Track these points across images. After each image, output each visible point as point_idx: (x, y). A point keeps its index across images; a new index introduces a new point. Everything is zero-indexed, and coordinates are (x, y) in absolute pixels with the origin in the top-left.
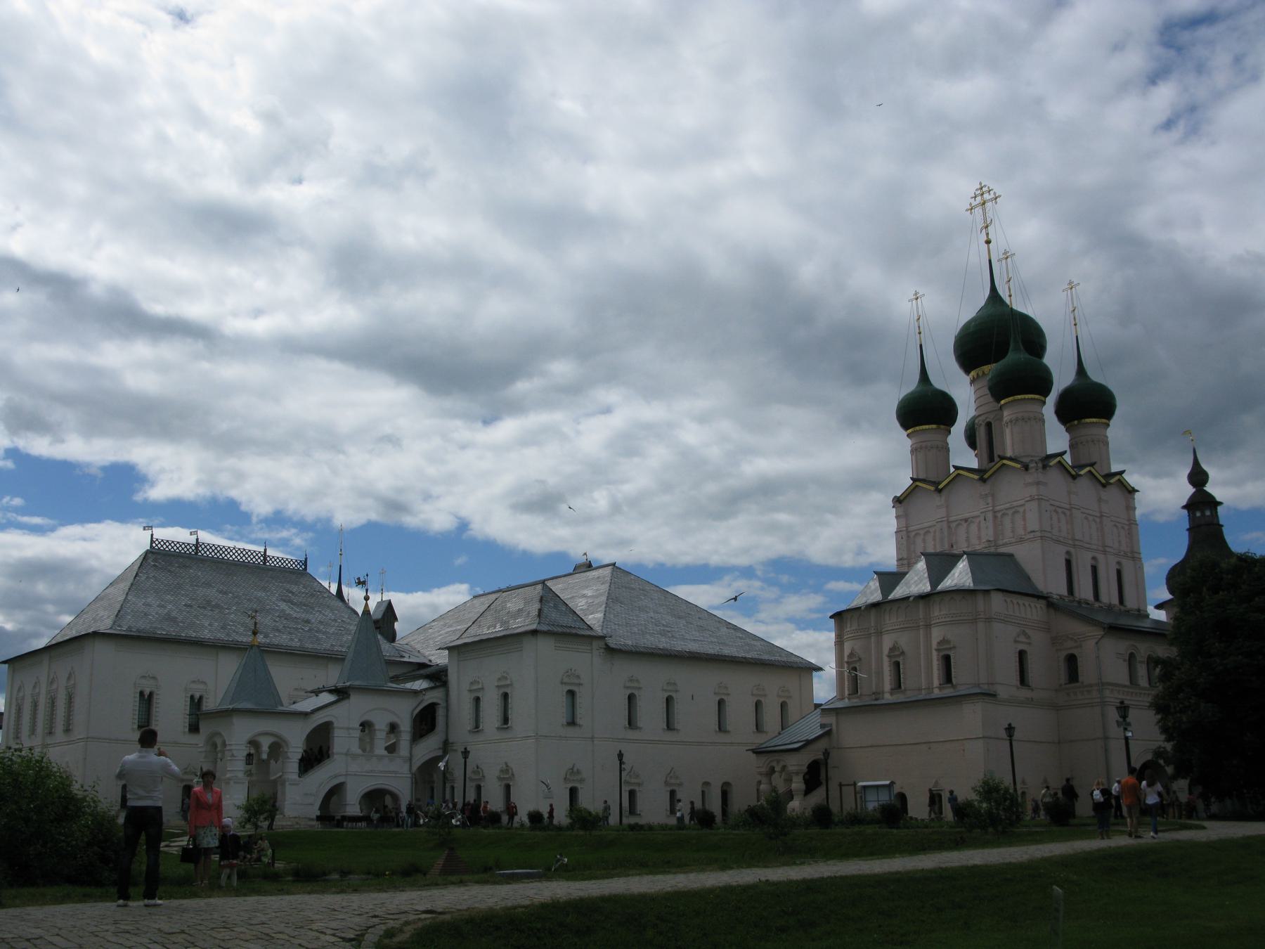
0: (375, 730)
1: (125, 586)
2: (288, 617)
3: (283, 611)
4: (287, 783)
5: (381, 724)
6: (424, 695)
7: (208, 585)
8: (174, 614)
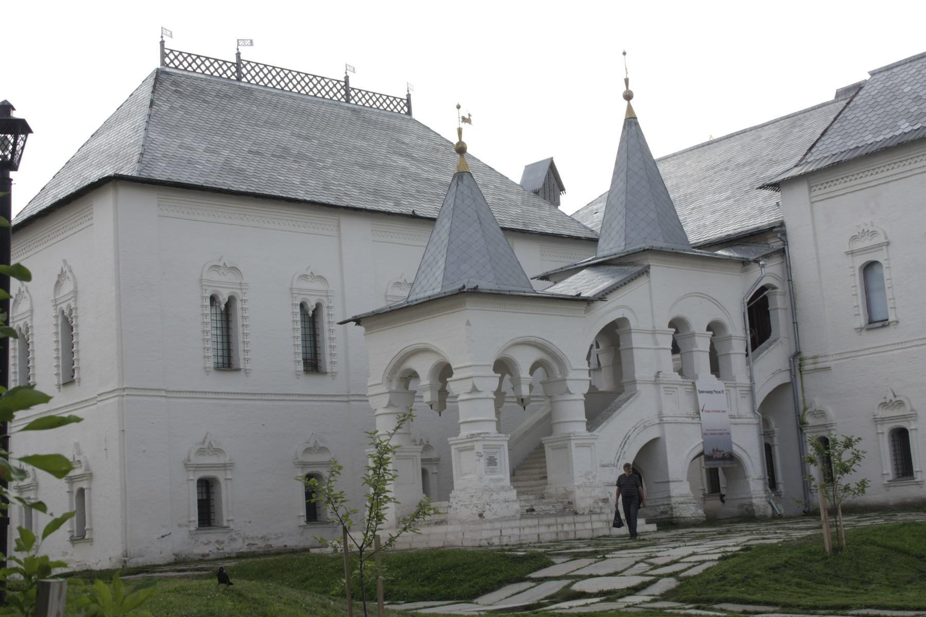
0: (693, 335)
1: (140, 119)
2: (416, 178)
3: (404, 168)
4: (573, 442)
5: (698, 325)
6: (763, 266)
7: (275, 125)
8: (237, 164)
